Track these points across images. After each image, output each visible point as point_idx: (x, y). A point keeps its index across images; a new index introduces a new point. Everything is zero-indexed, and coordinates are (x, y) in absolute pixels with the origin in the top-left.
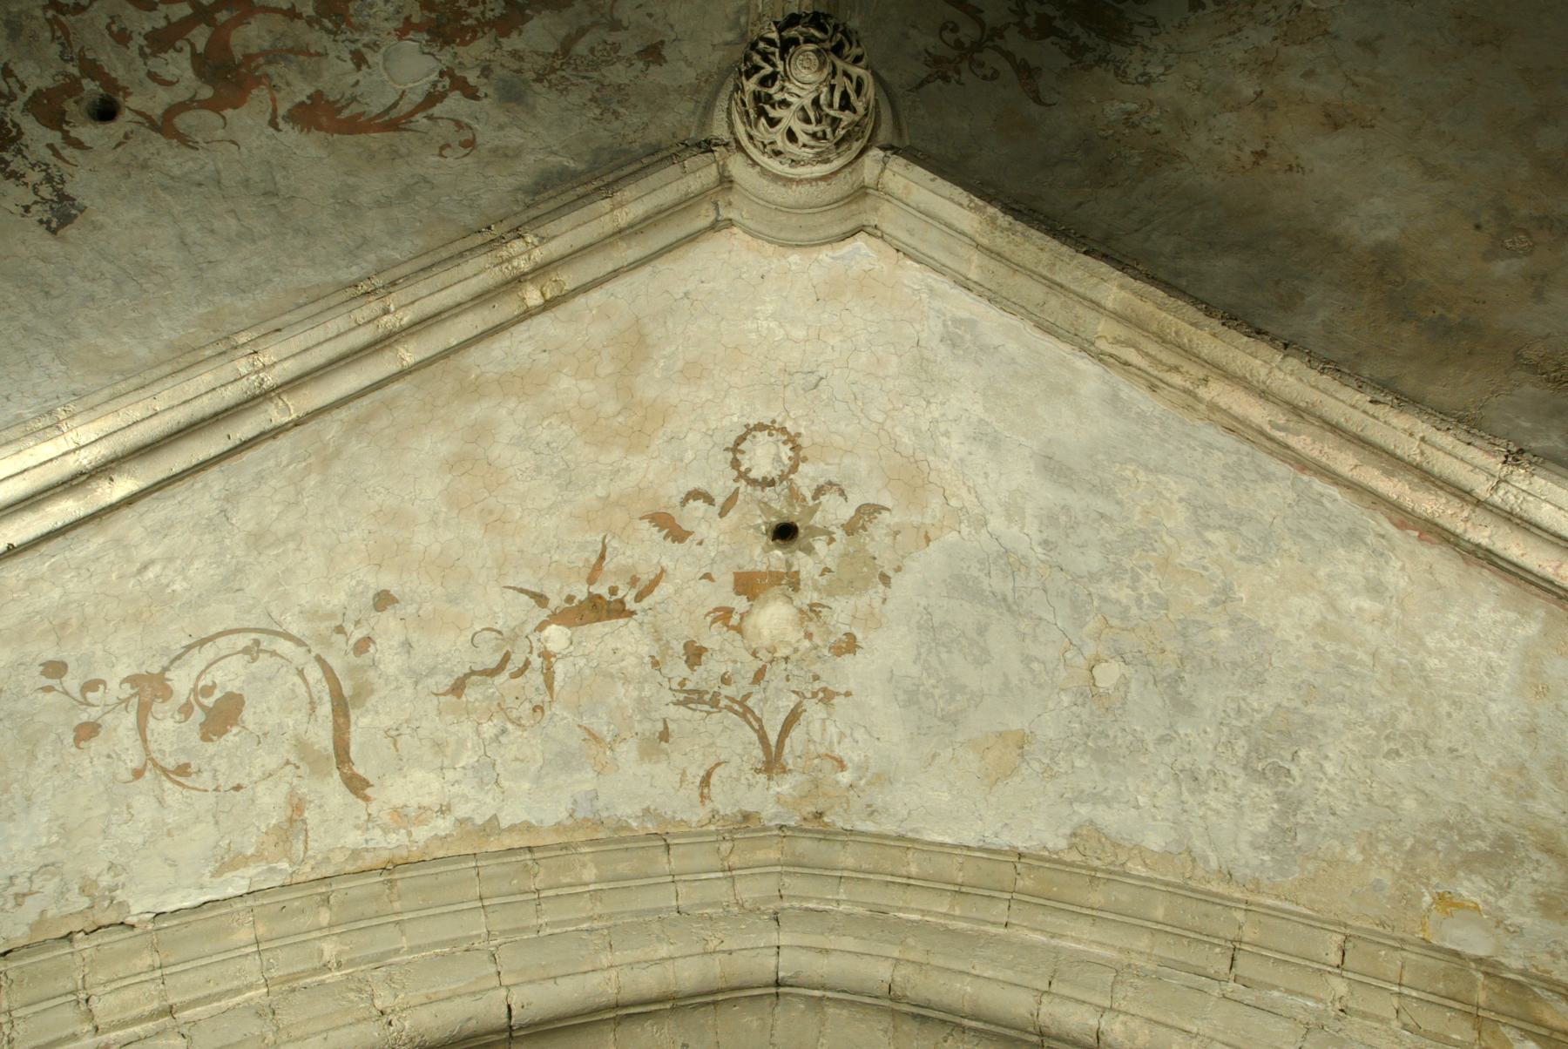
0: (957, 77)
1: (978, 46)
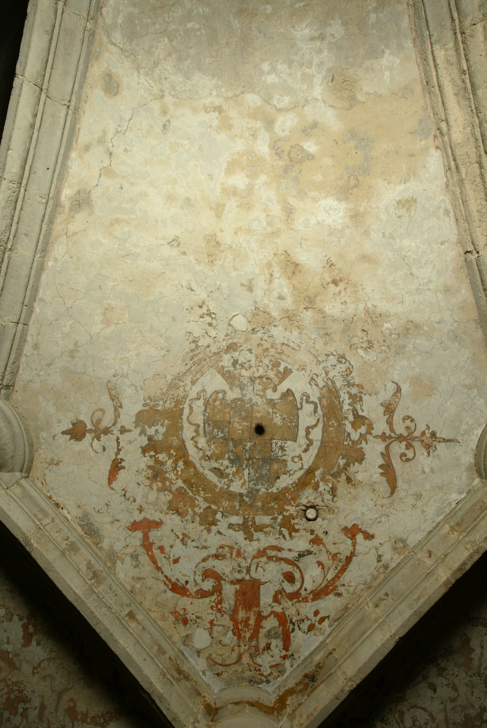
0: (427, 431)
1: (400, 438)
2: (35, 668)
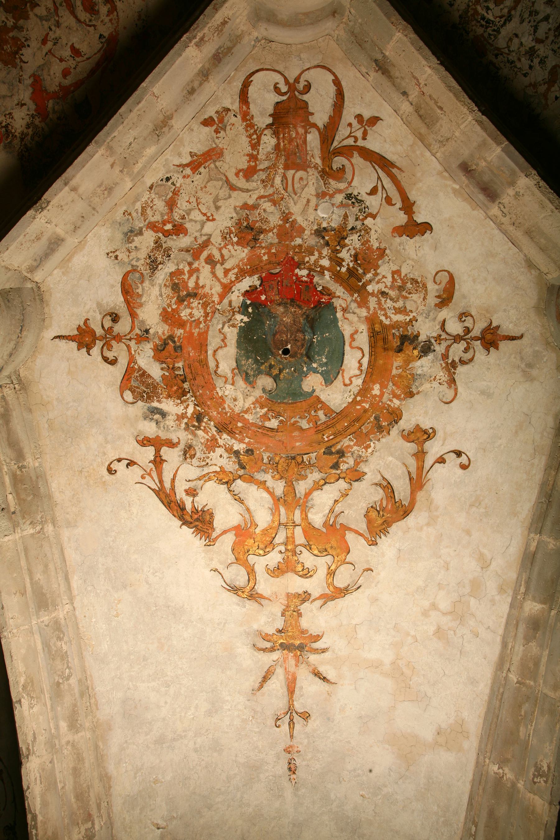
2: (208, 220)
